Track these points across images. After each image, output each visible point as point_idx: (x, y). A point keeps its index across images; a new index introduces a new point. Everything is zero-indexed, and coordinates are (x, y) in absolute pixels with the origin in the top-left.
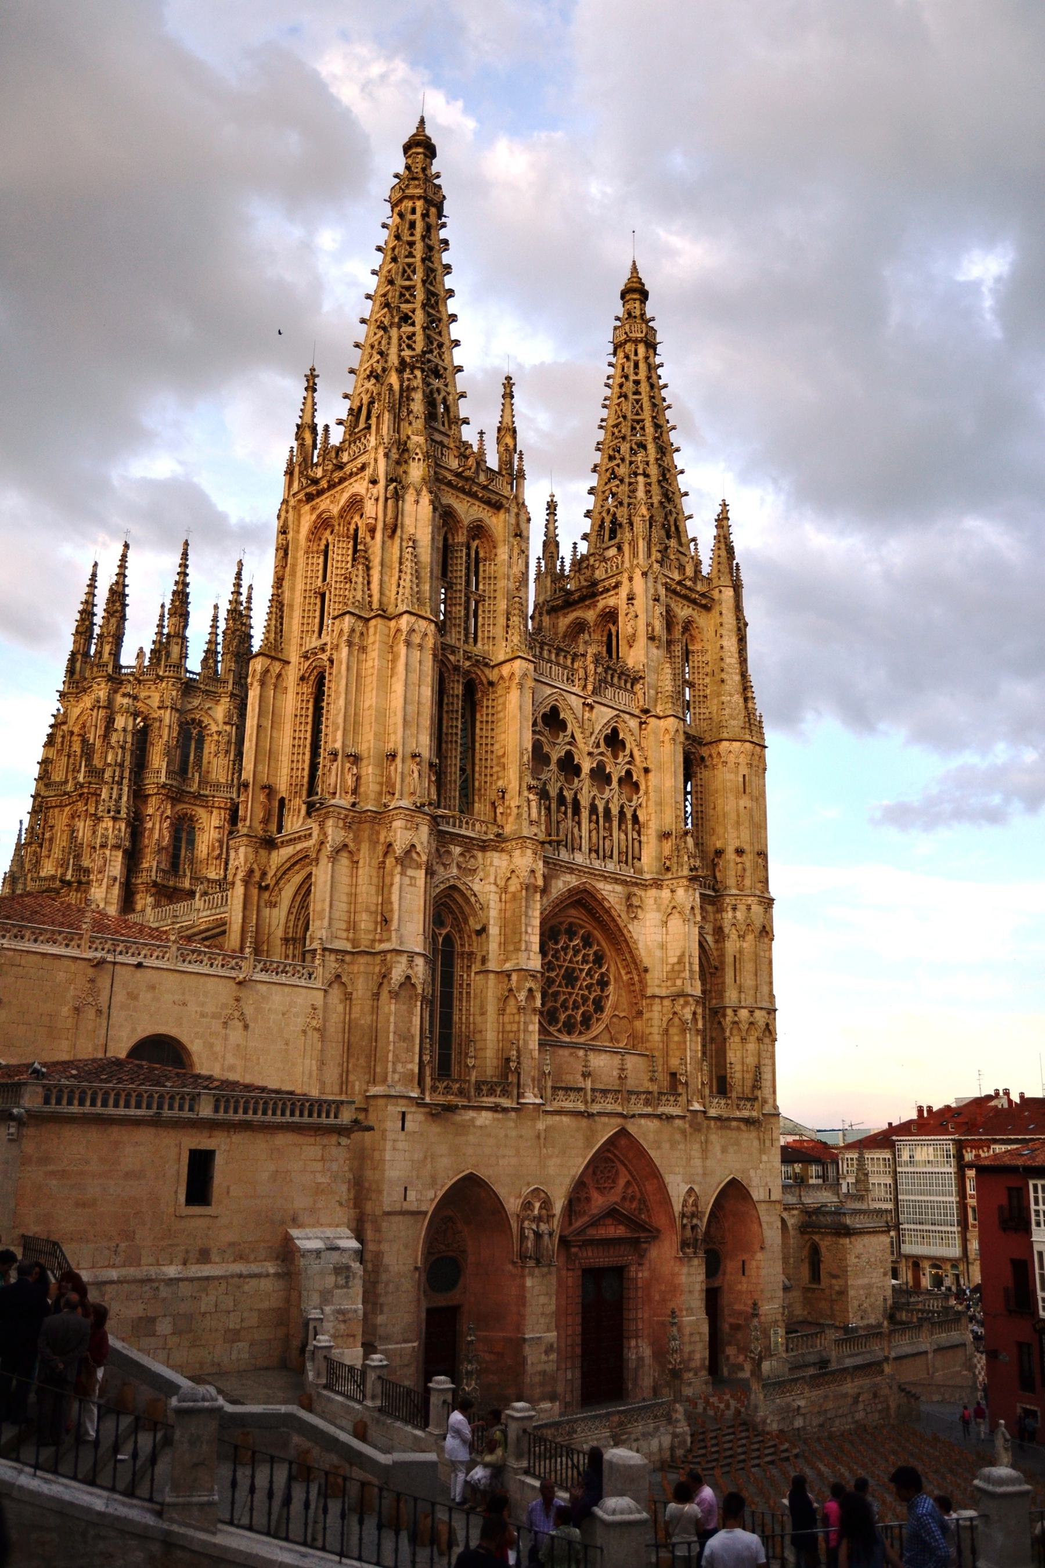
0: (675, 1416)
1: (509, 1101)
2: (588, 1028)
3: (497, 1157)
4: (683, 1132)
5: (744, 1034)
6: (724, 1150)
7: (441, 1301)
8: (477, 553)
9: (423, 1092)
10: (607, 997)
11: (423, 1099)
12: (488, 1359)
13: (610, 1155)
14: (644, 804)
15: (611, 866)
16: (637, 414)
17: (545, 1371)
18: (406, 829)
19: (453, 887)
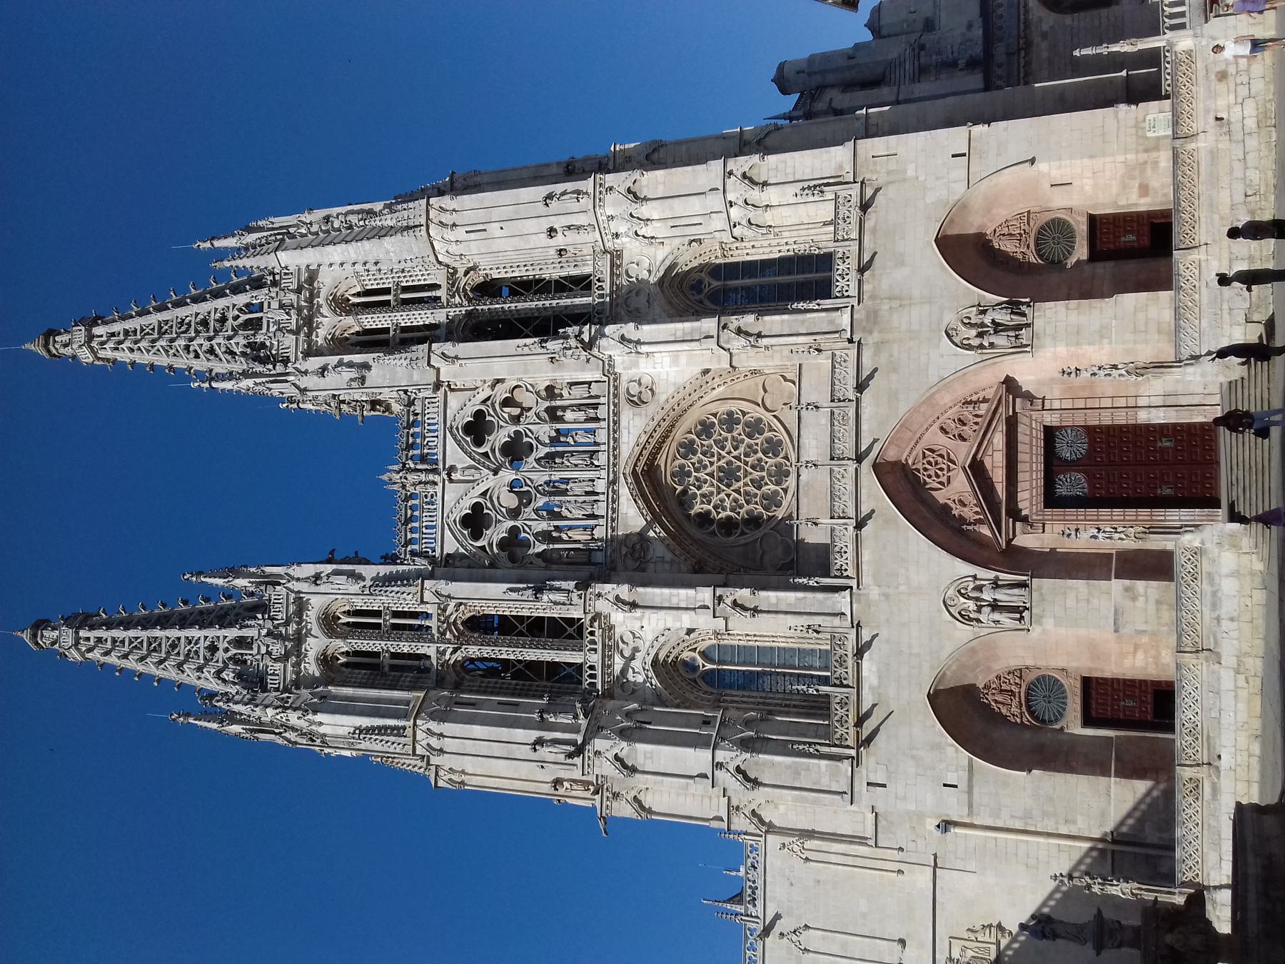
0: (1197, 544)
2: (780, 442)
3: (911, 654)
4: (879, 346)
5: (760, 211)
6: (901, 263)
8: (348, 613)
9: (847, 758)
10: (744, 414)
11: (853, 758)
12: (1142, 657)
14: (531, 381)
15: (602, 436)
16: (159, 350)
17: (1158, 602)
18: (601, 767)
19: (655, 663)
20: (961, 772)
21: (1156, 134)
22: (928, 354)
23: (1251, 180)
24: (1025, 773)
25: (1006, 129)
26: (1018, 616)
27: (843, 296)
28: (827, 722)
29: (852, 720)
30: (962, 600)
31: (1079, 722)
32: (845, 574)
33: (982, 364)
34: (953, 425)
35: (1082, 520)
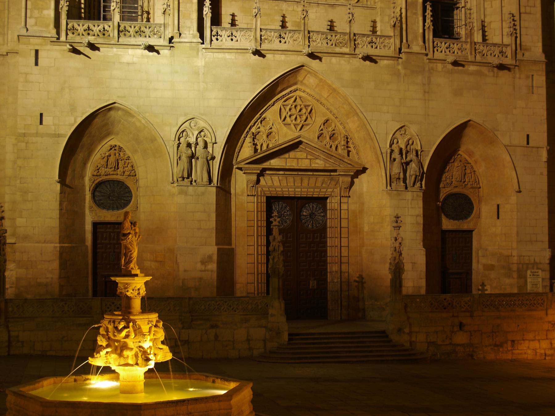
1: (162, 40)
6: (458, 93)
7: (109, 216)
9: (58, 33)
11: (58, 39)
13: (302, 94)
20: (53, 128)
21: (528, 276)
22: (388, 113)
23: (521, 344)
24: (57, 178)
25: (542, 174)
26: (186, 175)
27: (434, 47)
28: (83, 15)
29: (92, 39)
30: (196, 133)
31: (97, 219)
32: (214, 38)
33: (379, 152)
34: (330, 129)
35: (257, 224)
